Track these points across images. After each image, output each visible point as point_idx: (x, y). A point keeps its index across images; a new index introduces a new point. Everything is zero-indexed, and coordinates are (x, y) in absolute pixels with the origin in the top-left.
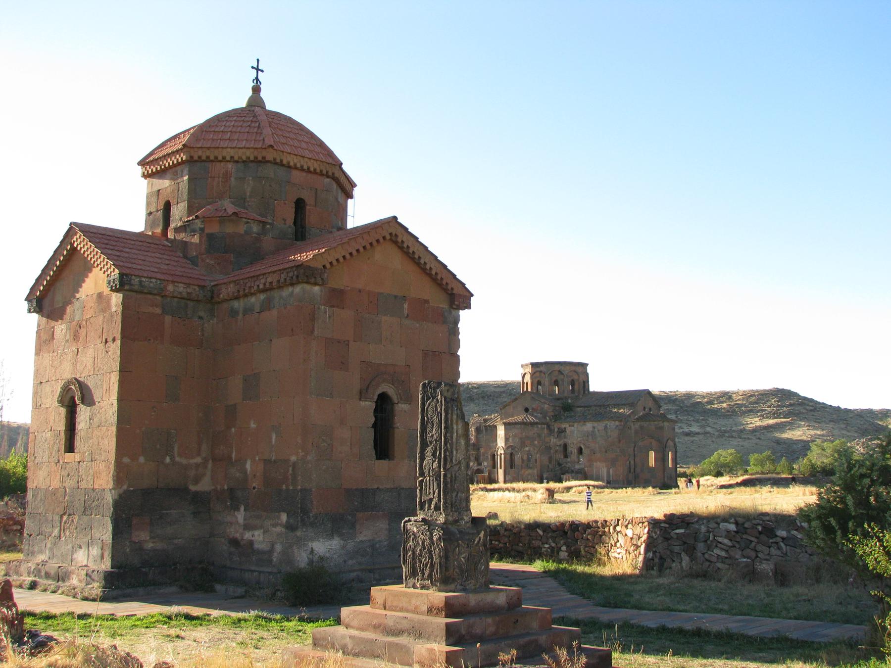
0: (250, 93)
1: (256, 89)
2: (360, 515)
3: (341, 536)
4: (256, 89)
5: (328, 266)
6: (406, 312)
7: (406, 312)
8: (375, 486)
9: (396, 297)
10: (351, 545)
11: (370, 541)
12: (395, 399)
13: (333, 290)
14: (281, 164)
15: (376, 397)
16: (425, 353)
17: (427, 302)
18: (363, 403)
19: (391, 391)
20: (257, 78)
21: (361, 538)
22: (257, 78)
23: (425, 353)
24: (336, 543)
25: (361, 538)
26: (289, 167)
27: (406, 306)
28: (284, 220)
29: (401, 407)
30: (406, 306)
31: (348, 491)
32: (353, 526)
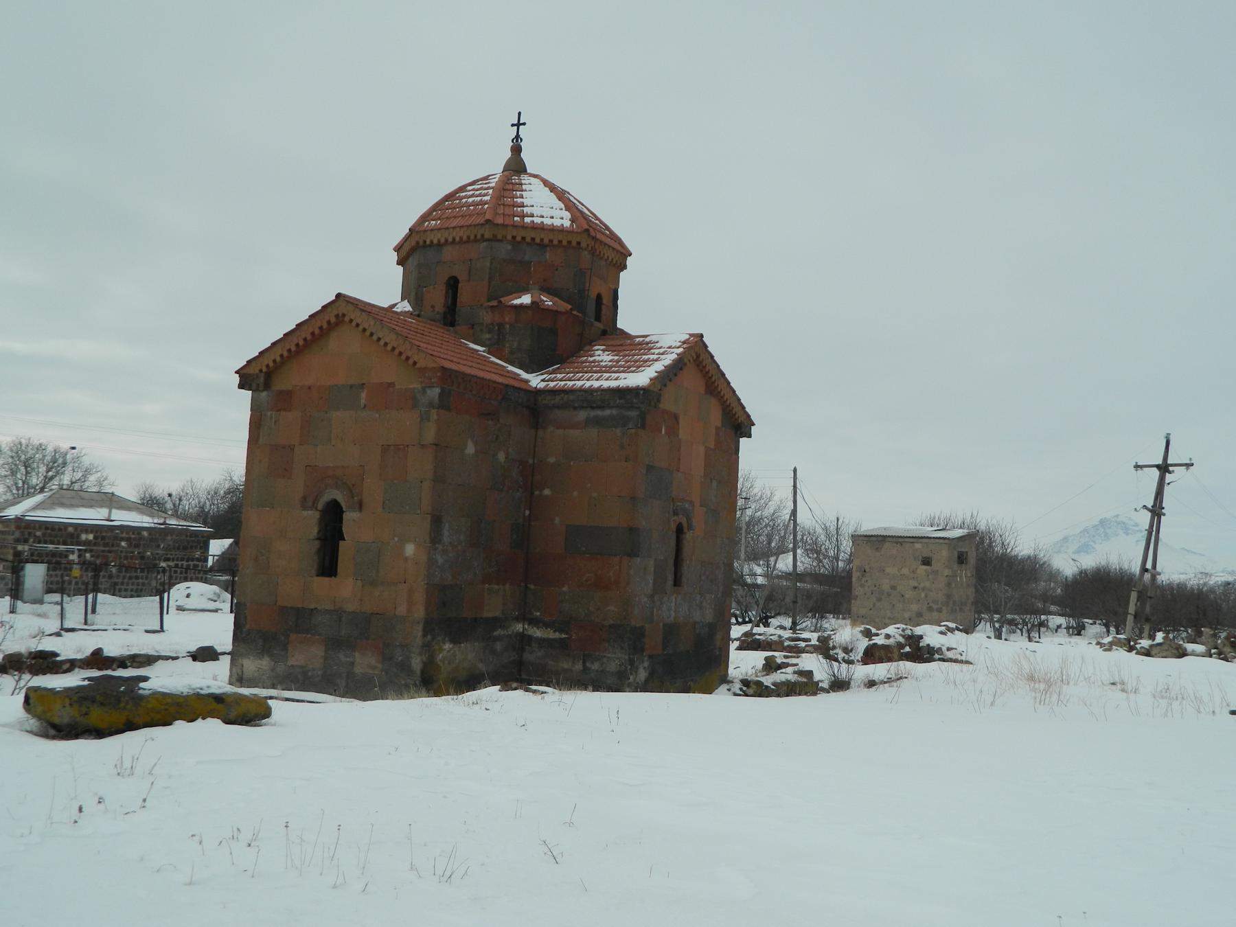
0: (509, 154)
1: (516, 149)
2: (293, 636)
3: (271, 656)
4: (516, 149)
5: (264, 369)
6: (363, 402)
7: (363, 402)
8: (313, 607)
9: (351, 386)
10: (281, 668)
11: (302, 667)
12: (343, 504)
13: (281, 392)
14: (425, 246)
15: (320, 506)
16: (385, 449)
17: (392, 384)
18: (305, 513)
19: (340, 497)
20: (518, 136)
21: (291, 662)
22: (518, 136)
23: (385, 449)
24: (265, 663)
25: (291, 662)
26: (439, 245)
27: (363, 395)
28: (433, 307)
29: (350, 516)
30: (363, 395)
31: (283, 608)
32: (285, 648)
